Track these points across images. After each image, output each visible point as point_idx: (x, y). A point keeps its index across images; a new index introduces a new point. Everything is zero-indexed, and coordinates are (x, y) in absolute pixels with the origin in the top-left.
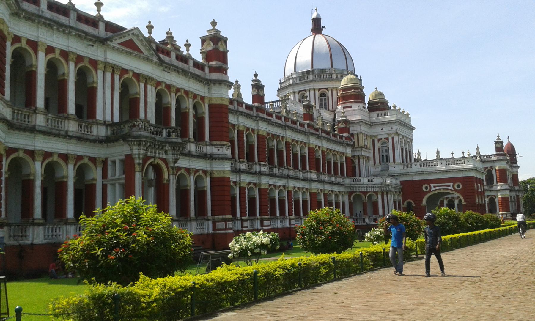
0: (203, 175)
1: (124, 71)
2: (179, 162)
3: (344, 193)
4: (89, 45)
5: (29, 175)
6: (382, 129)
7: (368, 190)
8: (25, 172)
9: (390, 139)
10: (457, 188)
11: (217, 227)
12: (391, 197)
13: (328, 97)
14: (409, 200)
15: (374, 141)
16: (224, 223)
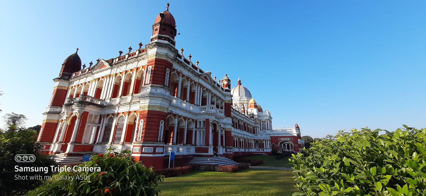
9: (266, 121)
11: (227, 151)
12: (268, 141)
14: (273, 143)
15: (260, 122)
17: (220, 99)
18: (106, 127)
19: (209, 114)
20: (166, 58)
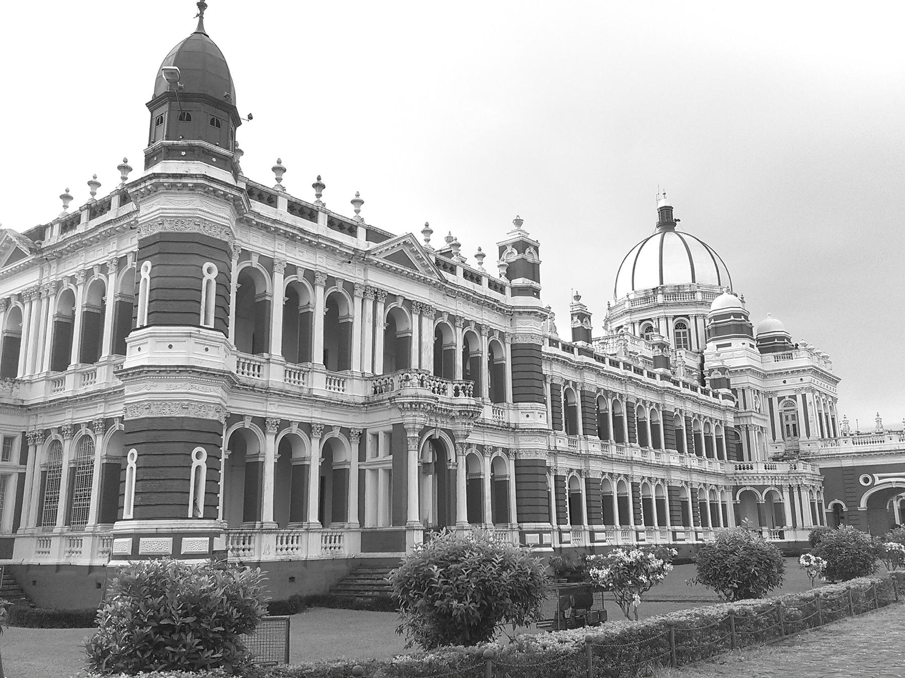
0: (504, 457)
1: (392, 297)
2: (471, 436)
3: (725, 487)
4: (344, 262)
5: (257, 455)
6: (785, 382)
7: (766, 484)
8: (250, 451)
9: (799, 397)
11: (528, 541)
12: (805, 495)
13: (689, 330)
14: (837, 501)
15: (770, 400)
16: (538, 535)
17: (483, 332)
18: (44, 474)
19: (401, 406)
20: (197, 227)
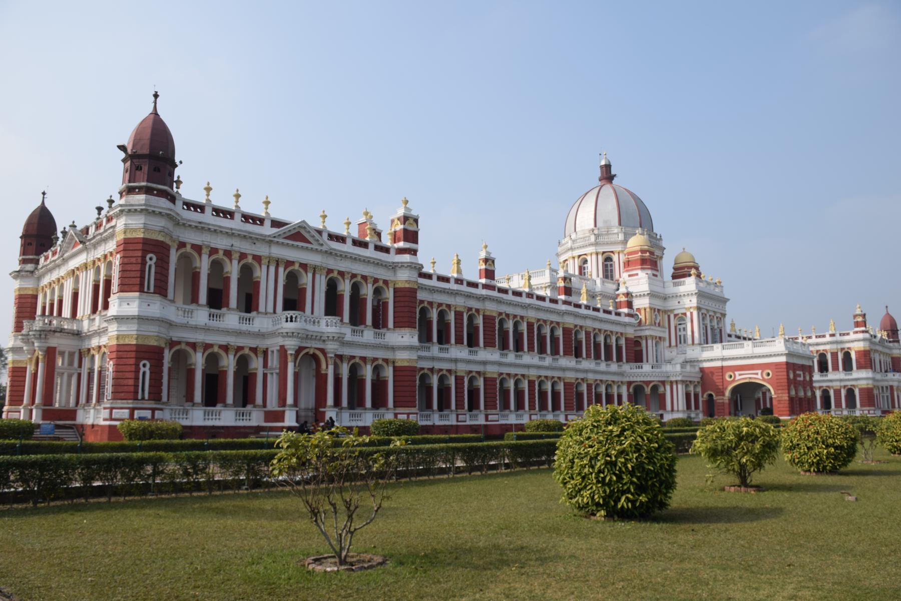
9: (688, 314)
10: (766, 377)
14: (710, 392)
15: (669, 317)
